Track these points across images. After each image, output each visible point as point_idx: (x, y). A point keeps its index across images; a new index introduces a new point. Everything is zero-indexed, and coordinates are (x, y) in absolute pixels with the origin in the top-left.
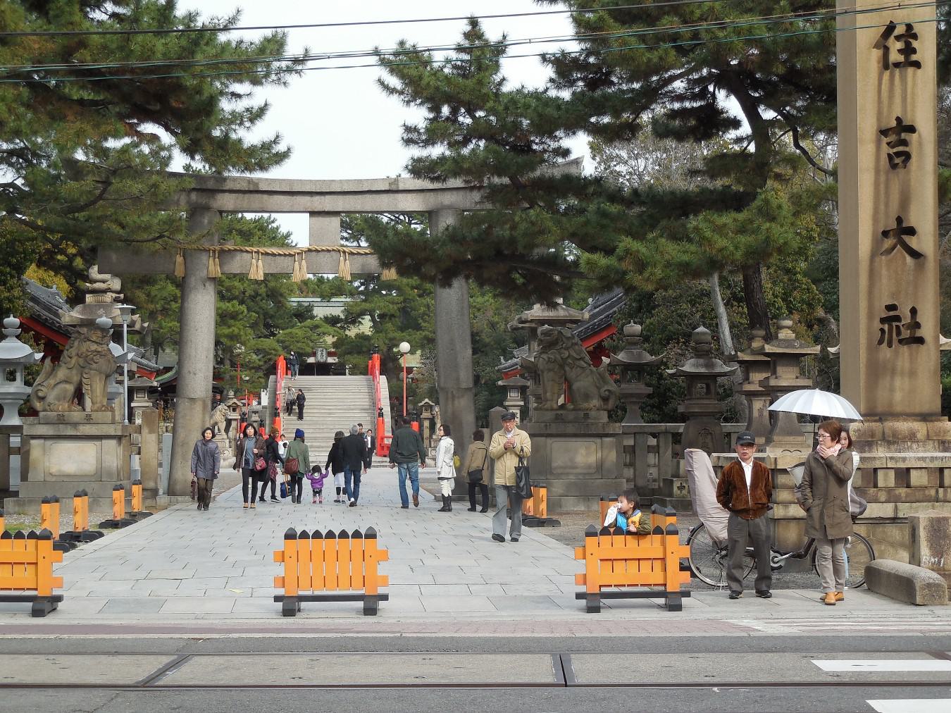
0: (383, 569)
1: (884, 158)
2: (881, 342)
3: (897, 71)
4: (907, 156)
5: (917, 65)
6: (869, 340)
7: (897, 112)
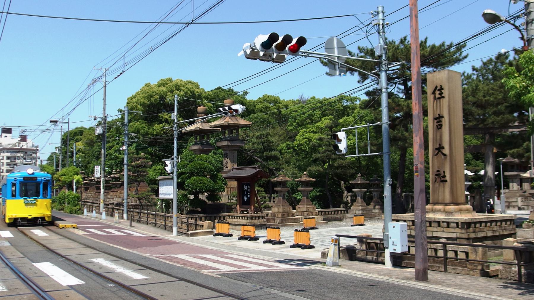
1: (435, 126)
2: (435, 182)
4: (441, 125)
7: (438, 113)
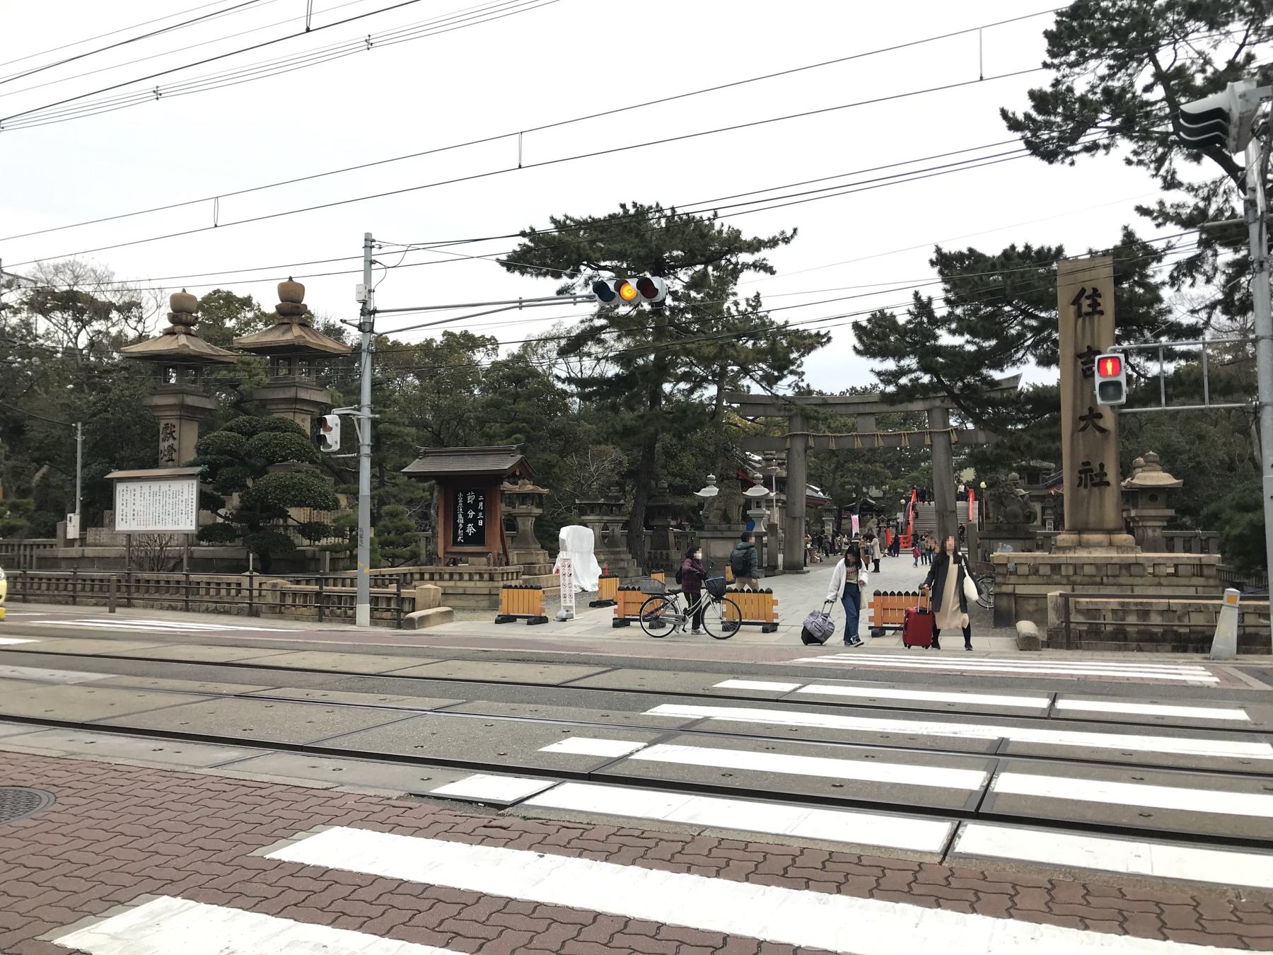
0: (776, 609)
1: (1079, 371)
2: (1079, 485)
3: (1087, 318)
5: (1101, 313)
6: (1072, 485)
7: (1088, 343)
